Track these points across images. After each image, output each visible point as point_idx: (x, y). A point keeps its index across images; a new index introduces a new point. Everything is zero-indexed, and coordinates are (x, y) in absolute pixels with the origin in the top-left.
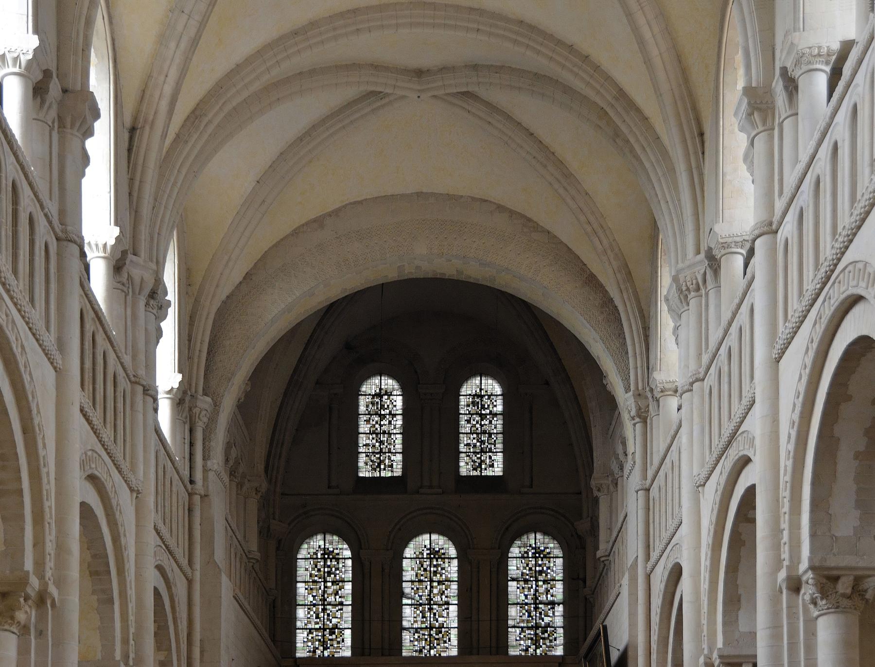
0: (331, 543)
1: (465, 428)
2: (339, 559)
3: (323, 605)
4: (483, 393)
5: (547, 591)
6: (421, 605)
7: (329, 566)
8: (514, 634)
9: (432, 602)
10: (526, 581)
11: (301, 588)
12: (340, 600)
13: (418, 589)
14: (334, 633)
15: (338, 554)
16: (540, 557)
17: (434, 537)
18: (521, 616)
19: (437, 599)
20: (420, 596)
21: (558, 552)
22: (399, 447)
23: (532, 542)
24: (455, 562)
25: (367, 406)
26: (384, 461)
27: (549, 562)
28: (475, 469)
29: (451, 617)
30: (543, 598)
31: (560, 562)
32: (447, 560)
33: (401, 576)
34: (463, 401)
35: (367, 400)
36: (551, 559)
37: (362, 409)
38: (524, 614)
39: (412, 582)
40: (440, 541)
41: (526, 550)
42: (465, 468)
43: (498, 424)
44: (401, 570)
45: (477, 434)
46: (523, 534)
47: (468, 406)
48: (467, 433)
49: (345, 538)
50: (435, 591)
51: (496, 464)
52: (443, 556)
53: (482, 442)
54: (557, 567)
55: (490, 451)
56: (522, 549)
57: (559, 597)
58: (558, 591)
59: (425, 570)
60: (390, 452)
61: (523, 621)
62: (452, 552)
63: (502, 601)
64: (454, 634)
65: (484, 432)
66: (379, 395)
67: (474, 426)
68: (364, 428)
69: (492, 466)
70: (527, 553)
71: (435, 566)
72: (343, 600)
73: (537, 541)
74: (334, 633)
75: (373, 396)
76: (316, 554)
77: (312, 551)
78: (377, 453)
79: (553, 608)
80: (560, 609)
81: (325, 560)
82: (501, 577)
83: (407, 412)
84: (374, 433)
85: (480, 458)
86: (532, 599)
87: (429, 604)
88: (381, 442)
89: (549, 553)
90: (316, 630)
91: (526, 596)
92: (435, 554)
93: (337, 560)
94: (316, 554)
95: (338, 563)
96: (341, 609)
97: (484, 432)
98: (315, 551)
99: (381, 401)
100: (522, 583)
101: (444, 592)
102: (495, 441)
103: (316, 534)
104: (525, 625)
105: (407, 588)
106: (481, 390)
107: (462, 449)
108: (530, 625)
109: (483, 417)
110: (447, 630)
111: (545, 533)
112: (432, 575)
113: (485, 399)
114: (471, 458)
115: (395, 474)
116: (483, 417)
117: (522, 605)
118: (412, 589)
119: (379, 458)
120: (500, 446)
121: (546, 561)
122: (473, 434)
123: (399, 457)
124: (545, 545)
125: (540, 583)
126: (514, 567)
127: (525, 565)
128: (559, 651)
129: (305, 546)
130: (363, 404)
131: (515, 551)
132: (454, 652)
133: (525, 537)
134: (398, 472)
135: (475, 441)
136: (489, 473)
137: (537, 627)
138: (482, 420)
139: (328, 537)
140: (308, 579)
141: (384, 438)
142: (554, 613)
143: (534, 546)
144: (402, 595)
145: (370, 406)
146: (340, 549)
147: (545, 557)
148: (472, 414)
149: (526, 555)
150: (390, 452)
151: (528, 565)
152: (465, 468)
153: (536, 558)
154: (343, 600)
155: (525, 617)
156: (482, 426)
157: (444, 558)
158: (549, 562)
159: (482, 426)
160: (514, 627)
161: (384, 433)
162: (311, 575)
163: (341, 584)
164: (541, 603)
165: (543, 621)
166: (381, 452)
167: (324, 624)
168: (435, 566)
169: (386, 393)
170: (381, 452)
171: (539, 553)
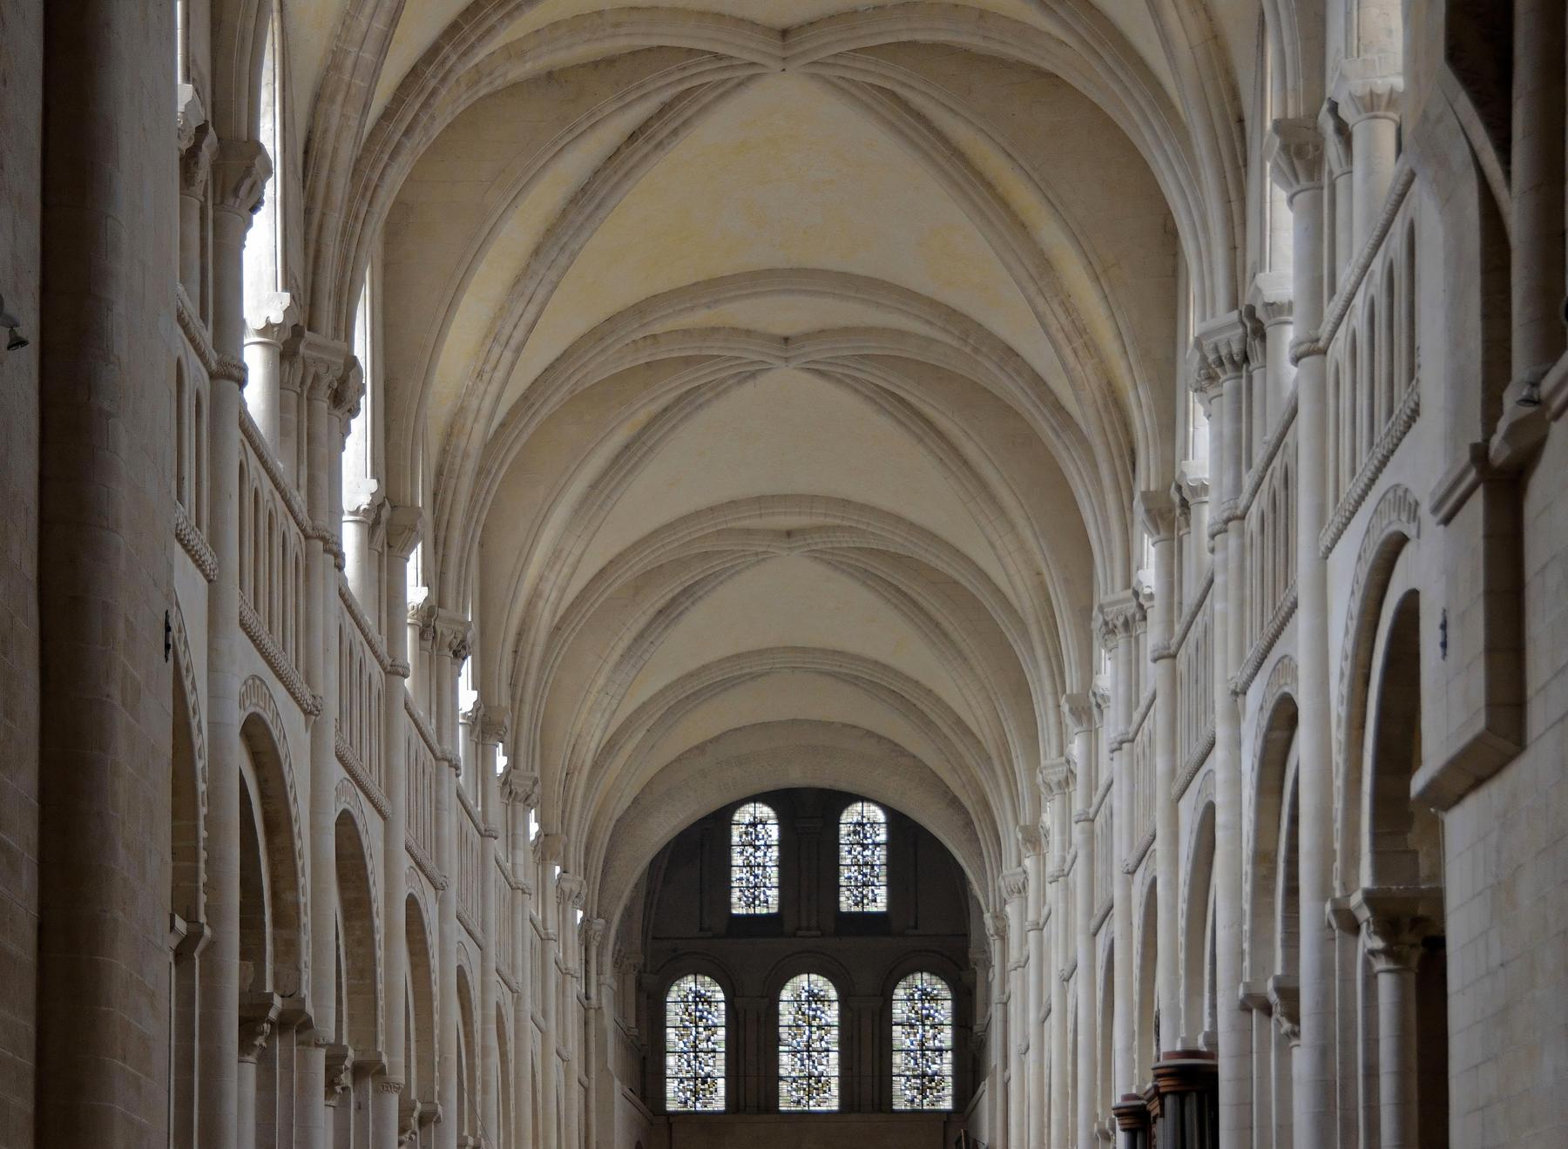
0: (703, 985)
1: (846, 858)
2: (711, 1002)
3: (695, 1052)
4: (865, 821)
5: (935, 1037)
6: (799, 1052)
8: (899, 1084)
9: (811, 1049)
10: (912, 1026)
11: (671, 1034)
12: (713, 1046)
13: (795, 1034)
14: (706, 1082)
15: (710, 997)
17: (813, 977)
18: (906, 1064)
19: (816, 1045)
21: (947, 994)
22: (775, 881)
24: (836, 1006)
25: (741, 837)
26: (758, 897)
27: (937, 1004)
28: (857, 904)
29: (831, 1066)
30: (930, 1044)
31: (948, 1004)
32: (826, 1003)
33: (777, 1020)
34: (844, 830)
37: (735, 839)
39: (790, 1027)
40: (819, 983)
42: (846, 903)
43: (880, 855)
44: (777, 1014)
46: (908, 974)
47: (849, 835)
48: (847, 865)
49: (717, 980)
51: (878, 899)
53: (865, 875)
54: (944, 1011)
55: (873, 884)
56: (908, 991)
57: (948, 1043)
58: (946, 1036)
59: (803, 1014)
60: (765, 886)
61: (908, 1069)
62: (833, 994)
63: (885, 1047)
64: (834, 1083)
65: (866, 864)
66: (754, 825)
67: (855, 857)
68: (737, 860)
69: (875, 901)
71: (813, 1010)
72: (716, 1047)
74: (706, 1082)
75: (747, 826)
76: (686, 996)
77: (682, 993)
78: (752, 888)
79: (941, 1055)
80: (948, 1056)
82: (884, 1020)
83: (783, 844)
84: (748, 865)
85: (862, 893)
87: (808, 1051)
88: (756, 876)
89: (937, 995)
90: (688, 1079)
92: (814, 997)
93: (710, 1003)
94: (686, 996)
95: (710, 1007)
96: (714, 1057)
97: (866, 864)
99: (756, 830)
100: (907, 1028)
101: (823, 1037)
102: (878, 874)
103: (686, 975)
104: (911, 1073)
105: (784, 1033)
106: (863, 817)
107: (843, 881)
108: (916, 1073)
109: (865, 847)
111: (932, 973)
113: (867, 828)
114: (852, 892)
115: (771, 911)
116: (865, 847)
117: (908, 1052)
118: (790, 1034)
119: (754, 893)
120: (883, 879)
122: (854, 866)
123: (775, 892)
125: (927, 1028)
126: (900, 1010)
127: (911, 1008)
128: (947, 1105)
129: (675, 988)
131: (900, 993)
132: (833, 1105)
133: (911, 977)
134: (774, 909)
135: (856, 874)
136: (871, 908)
137: (924, 1075)
138: (864, 850)
139: (700, 978)
140: (678, 1024)
141: (759, 871)
142: (941, 1060)
144: (777, 1040)
145: (744, 836)
146: (713, 991)
147: (932, 999)
148: (853, 844)
149: (911, 997)
150: (765, 886)
151: (913, 1008)
152: (846, 903)
153: (922, 1000)
154: (716, 1047)
156: (864, 857)
157: (824, 1001)
158: (937, 1004)
159: (864, 857)
160: (899, 1075)
161: (759, 865)
162: (682, 1020)
163: (713, 1029)
165: (930, 1068)
166: (755, 886)
169: (761, 822)
170: (755, 886)
171: (926, 996)
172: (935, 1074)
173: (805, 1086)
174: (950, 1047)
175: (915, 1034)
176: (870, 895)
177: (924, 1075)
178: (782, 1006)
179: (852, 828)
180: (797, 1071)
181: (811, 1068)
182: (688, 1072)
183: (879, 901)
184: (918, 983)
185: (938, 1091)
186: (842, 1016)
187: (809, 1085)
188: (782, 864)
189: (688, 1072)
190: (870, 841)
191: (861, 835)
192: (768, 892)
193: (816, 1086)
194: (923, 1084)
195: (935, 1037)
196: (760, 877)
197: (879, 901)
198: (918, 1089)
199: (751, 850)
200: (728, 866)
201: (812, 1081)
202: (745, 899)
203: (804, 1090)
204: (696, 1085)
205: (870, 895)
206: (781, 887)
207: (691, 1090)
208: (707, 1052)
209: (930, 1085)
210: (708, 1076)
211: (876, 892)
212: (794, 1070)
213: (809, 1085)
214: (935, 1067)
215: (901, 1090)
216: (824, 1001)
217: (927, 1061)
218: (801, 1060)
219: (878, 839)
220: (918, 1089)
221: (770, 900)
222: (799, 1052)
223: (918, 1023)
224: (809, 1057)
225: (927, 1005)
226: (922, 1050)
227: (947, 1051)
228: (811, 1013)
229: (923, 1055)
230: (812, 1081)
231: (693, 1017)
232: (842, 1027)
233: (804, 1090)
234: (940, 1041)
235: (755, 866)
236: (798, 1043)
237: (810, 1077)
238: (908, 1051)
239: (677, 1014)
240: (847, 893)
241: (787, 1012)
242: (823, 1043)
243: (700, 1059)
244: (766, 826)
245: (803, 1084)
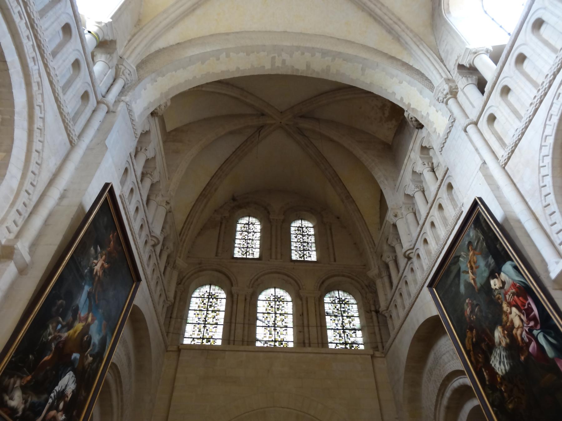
0: (214, 290)
2: (218, 298)
3: (205, 324)
4: (303, 226)
5: (350, 323)
6: (269, 326)
7: (211, 302)
9: (276, 326)
10: (336, 316)
11: (191, 314)
12: (216, 321)
13: (267, 317)
14: (209, 341)
15: (218, 296)
16: (342, 303)
17: (278, 290)
18: (335, 337)
20: (269, 322)
22: (258, 246)
23: (337, 295)
24: (290, 304)
25: (241, 228)
26: (249, 251)
27: (349, 306)
28: (300, 258)
32: (285, 302)
33: (256, 310)
35: (242, 226)
36: (350, 305)
38: (336, 335)
39: (263, 313)
41: (334, 299)
44: (256, 306)
45: (301, 243)
46: (331, 291)
47: (295, 231)
48: (295, 242)
50: (278, 319)
51: (312, 256)
52: (283, 300)
53: (304, 246)
55: (308, 250)
56: (332, 299)
59: (272, 307)
60: (252, 247)
61: (337, 339)
65: (305, 242)
66: (248, 224)
67: (299, 239)
68: (238, 236)
69: (310, 257)
70: (334, 300)
71: (278, 305)
72: (217, 321)
73: (340, 295)
74: (209, 341)
75: (245, 224)
76: (204, 295)
77: (201, 294)
78: (245, 248)
79: (355, 332)
81: (209, 298)
82: (321, 315)
83: (262, 231)
84: (244, 239)
85: (303, 253)
86: (341, 326)
87: (275, 327)
88: (248, 243)
89: (348, 301)
90: (197, 338)
91: (337, 324)
92: (277, 299)
93: (217, 299)
94: (204, 295)
95: (217, 301)
96: (216, 327)
97: (305, 242)
98: (203, 293)
99: (249, 226)
100: (333, 317)
101: (283, 320)
102: (311, 246)
103: (205, 285)
104: (338, 342)
105: (260, 316)
106: (302, 225)
107: (293, 248)
108: (341, 342)
109: (303, 236)
110: (286, 342)
112: (276, 310)
113: (304, 229)
114: (298, 253)
115: (255, 257)
116: (303, 236)
118: (263, 317)
119: (246, 250)
120: (314, 249)
121: (346, 306)
122: (298, 242)
124: (345, 297)
125: (345, 318)
126: (328, 308)
127: (334, 307)
129: (198, 291)
130: (239, 227)
131: (327, 299)
133: (333, 292)
134: (257, 255)
135: (300, 245)
136: (309, 259)
137: (346, 343)
138: (303, 237)
139: (213, 287)
140: (197, 308)
141: (250, 242)
142: (356, 335)
143: (338, 297)
145: (243, 228)
146: (219, 293)
147: (346, 303)
148: (298, 234)
149: (334, 302)
150: (252, 247)
151: (336, 307)
153: (340, 304)
154: (217, 321)
155: (338, 337)
156: (303, 239)
157: (284, 301)
158: (349, 306)
159: (303, 239)
160: (331, 343)
161: (250, 239)
162: (199, 307)
163: (217, 312)
164: (347, 329)
165: (350, 340)
166: (247, 247)
167: (203, 336)
168: (278, 305)
169: (252, 223)
170: (247, 247)
176: (308, 254)
178: (259, 303)
179: (297, 228)
182: (198, 335)
184: (337, 295)
188: (262, 239)
190: (306, 234)
191: (302, 231)
192: (254, 250)
196: (250, 244)
197: (314, 257)
200: (234, 239)
202: (242, 252)
205: (308, 254)
211: (310, 253)
214: (352, 340)
216: (284, 301)
219: (309, 233)
221: (255, 253)
223: (339, 315)
225: (343, 306)
226: (343, 329)
228: (276, 307)
231: (206, 306)
235: (248, 239)
239: (196, 303)
240: (296, 253)
241: (262, 306)
242: (283, 323)
244: (254, 225)
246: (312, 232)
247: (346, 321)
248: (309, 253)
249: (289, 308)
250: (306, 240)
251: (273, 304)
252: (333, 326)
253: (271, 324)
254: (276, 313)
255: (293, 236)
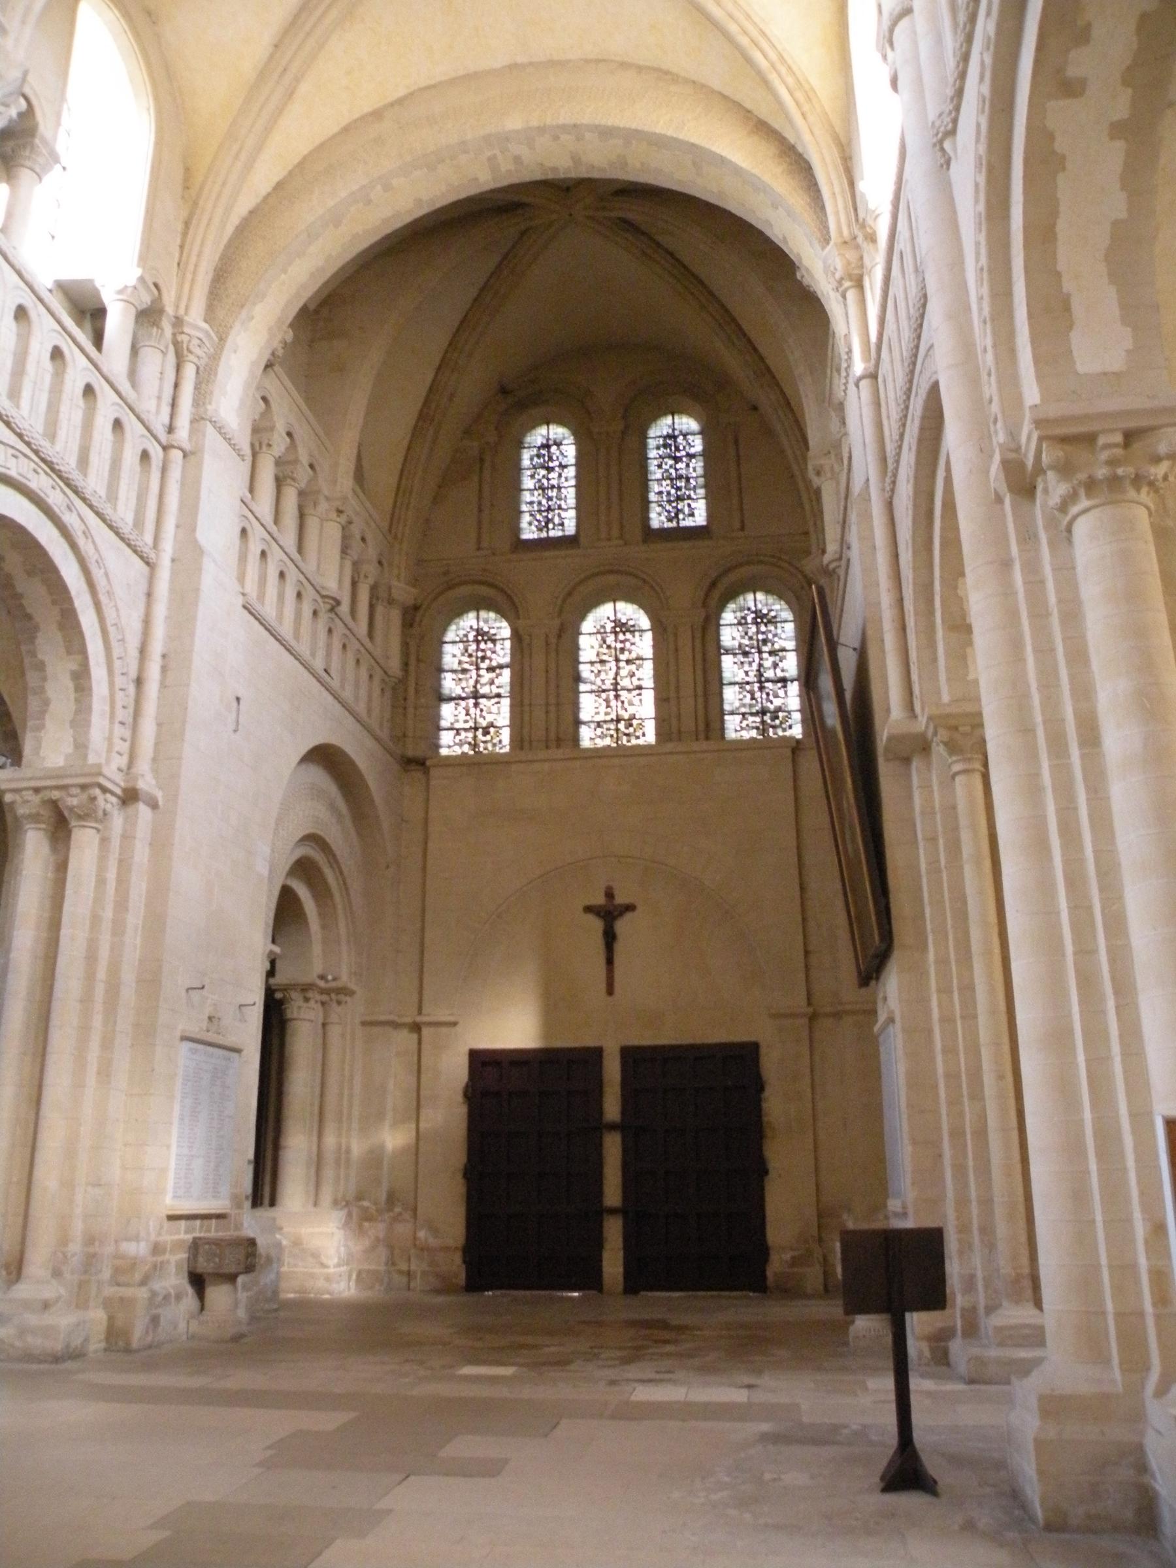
0: (486, 621)
5: (775, 665)
6: (604, 691)
7: (483, 651)
9: (619, 687)
10: (746, 654)
13: (599, 671)
14: (488, 733)
15: (495, 635)
16: (762, 622)
17: (621, 605)
18: (741, 700)
20: (603, 681)
21: (787, 614)
23: (751, 604)
24: (649, 636)
25: (532, 459)
27: (776, 628)
28: (670, 520)
30: (769, 674)
35: (532, 453)
36: (779, 625)
38: (745, 696)
39: (592, 663)
40: (629, 611)
41: (743, 615)
44: (576, 648)
45: (672, 480)
50: (623, 673)
51: (696, 512)
52: (632, 629)
53: (678, 489)
54: (786, 634)
55: (689, 497)
56: (739, 614)
59: (609, 647)
60: (560, 508)
61: (744, 705)
65: (680, 477)
66: (546, 446)
67: (667, 471)
69: (692, 515)
70: (744, 618)
71: (622, 642)
73: (758, 603)
74: (488, 733)
75: (539, 448)
76: (466, 636)
77: (461, 633)
79: (785, 687)
81: (478, 642)
84: (540, 488)
85: (676, 507)
88: (550, 499)
89: (775, 617)
90: (466, 730)
91: (747, 673)
92: (621, 627)
93: (494, 641)
94: (466, 636)
95: (495, 645)
96: (498, 703)
97: (680, 477)
98: (465, 632)
100: (741, 658)
105: (585, 671)
106: (674, 430)
107: (653, 497)
108: (754, 710)
110: (640, 721)
112: (618, 653)
113: (680, 439)
115: (567, 533)
116: (677, 460)
117: (742, 685)
121: (771, 627)
124: (769, 608)
125: (765, 655)
126: (729, 636)
127: (743, 634)
129: (453, 627)
131: (728, 617)
133: (741, 598)
136: (688, 522)
137: (763, 712)
139: (483, 614)
141: (553, 493)
142: (786, 693)
143: (754, 609)
144: (578, 679)
145: (536, 459)
146: (498, 628)
147: (770, 622)
149: (743, 621)
153: (757, 624)
155: (747, 700)
156: (676, 470)
158: (776, 628)
159: (676, 470)
161: (553, 487)
162: (460, 663)
164: (768, 680)
165: (771, 702)
166: (549, 509)
167: (475, 723)
168: (622, 642)
170: (549, 509)
172: (779, 709)
173: (612, 732)
174: (796, 677)
175: (750, 664)
176: (686, 510)
177: (763, 712)
178: (584, 641)
179: (661, 442)
180: (602, 714)
181: (764, 701)
182: (466, 721)
183: (698, 514)
184: (751, 604)
185: (784, 730)
186: (656, 646)
187: (617, 730)
189: (466, 721)
190: (683, 453)
191: (673, 448)
192: (563, 514)
193: (627, 731)
194: (763, 722)
195: (775, 665)
196: (555, 500)
197: (698, 514)
198: (757, 728)
199: (543, 472)
200: (518, 489)
201: (622, 726)
202: (536, 523)
203: (612, 736)
204: (475, 737)
205: (686, 510)
206: (578, 508)
207: (469, 744)
208: (774, 682)
209: (773, 723)
210: (492, 725)
211: (693, 505)
212: (597, 713)
213: (617, 730)
214: (777, 702)
215: (736, 731)
217: (768, 694)
218: (607, 701)
219: (692, 451)
220: (757, 728)
221: (566, 522)
222: (604, 691)
223: (753, 651)
224: (617, 697)
225: (763, 628)
226: (760, 682)
227: (792, 681)
228: (619, 645)
229: (761, 688)
230: (622, 726)
231: (474, 659)
232: (657, 659)
233: (612, 736)
234: (783, 671)
235: (548, 488)
236: (603, 681)
237: (618, 720)
238: (598, 691)
239: (454, 656)
240: (659, 509)
241: (588, 647)
242: (634, 679)
243: (767, 690)
244: (561, 447)
245: (608, 729)
246: (698, 445)
247: (768, 662)
248: (689, 505)
249: (644, 645)
250: (683, 472)
251: (610, 639)
252: (740, 676)
253: (608, 685)
254: (617, 660)
255: (653, 465)
